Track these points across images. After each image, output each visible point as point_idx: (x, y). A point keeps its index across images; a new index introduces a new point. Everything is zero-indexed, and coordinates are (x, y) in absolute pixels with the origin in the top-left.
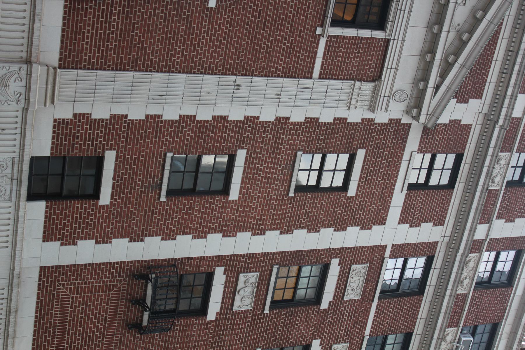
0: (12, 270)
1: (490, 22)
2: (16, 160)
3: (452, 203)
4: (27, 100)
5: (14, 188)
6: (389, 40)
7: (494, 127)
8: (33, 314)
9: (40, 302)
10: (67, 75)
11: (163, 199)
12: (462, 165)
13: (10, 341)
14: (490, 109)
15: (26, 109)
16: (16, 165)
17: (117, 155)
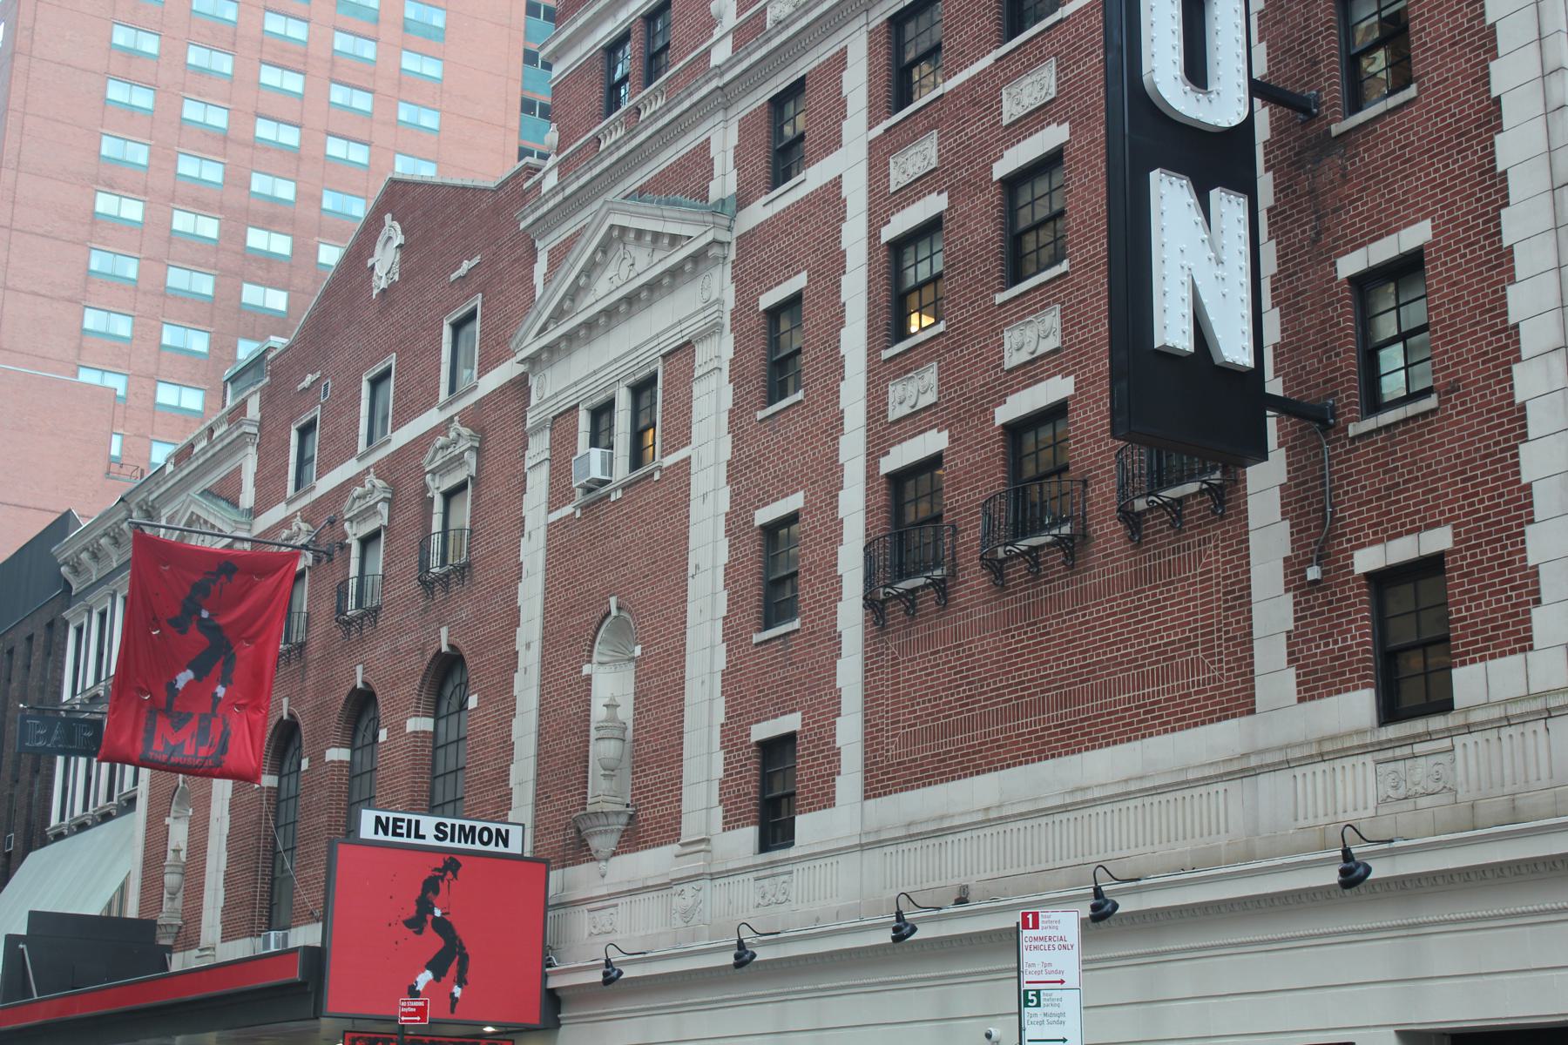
0: (862, 847)
1: (632, 214)
2: (755, 875)
3: (821, 60)
4: (697, 877)
5: (780, 870)
6: (663, 356)
7: (726, 85)
8: (941, 787)
9: (907, 786)
10: (691, 827)
11: (796, 624)
12: (781, 88)
13: (946, 824)
14: (713, 112)
15: (713, 877)
16: (762, 874)
17: (758, 722)
